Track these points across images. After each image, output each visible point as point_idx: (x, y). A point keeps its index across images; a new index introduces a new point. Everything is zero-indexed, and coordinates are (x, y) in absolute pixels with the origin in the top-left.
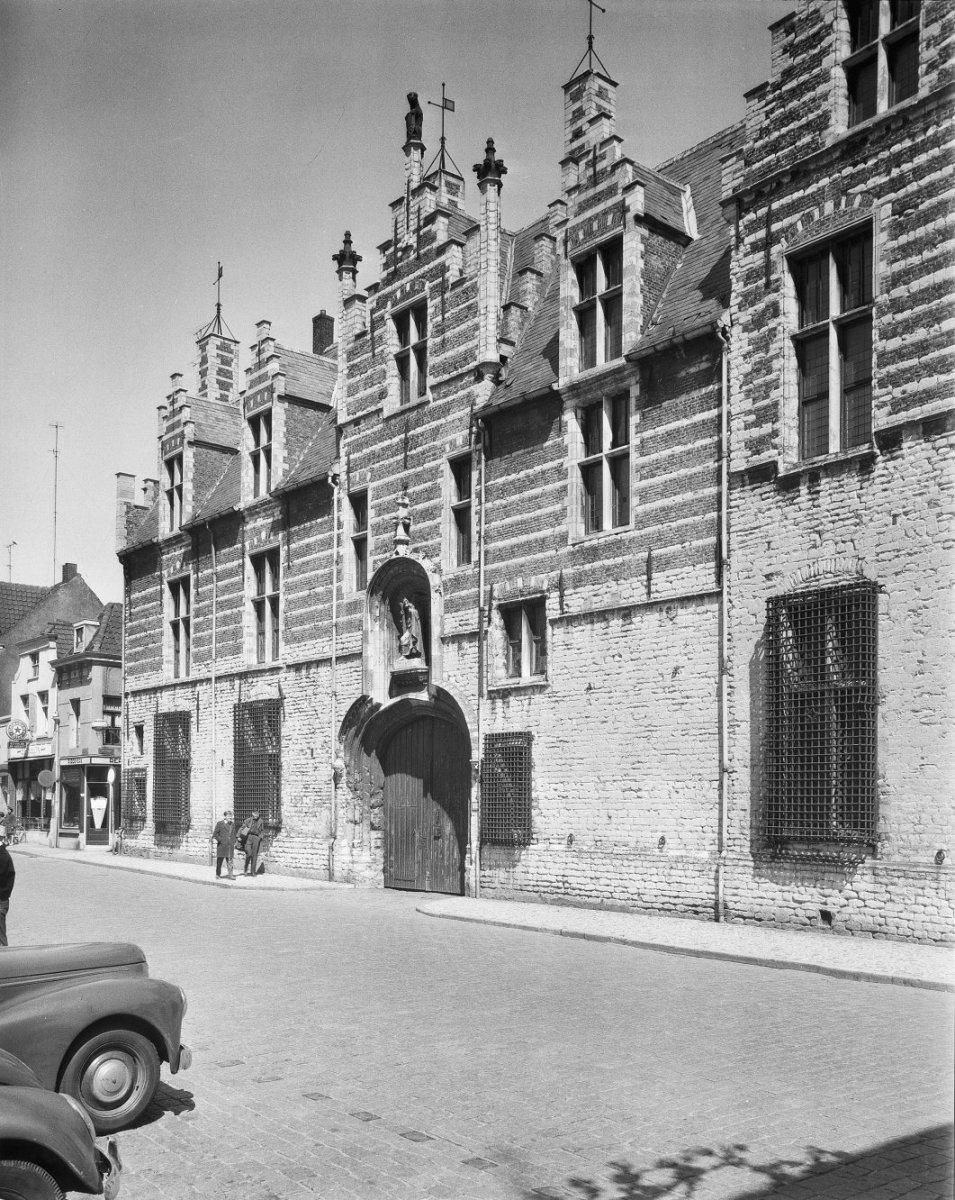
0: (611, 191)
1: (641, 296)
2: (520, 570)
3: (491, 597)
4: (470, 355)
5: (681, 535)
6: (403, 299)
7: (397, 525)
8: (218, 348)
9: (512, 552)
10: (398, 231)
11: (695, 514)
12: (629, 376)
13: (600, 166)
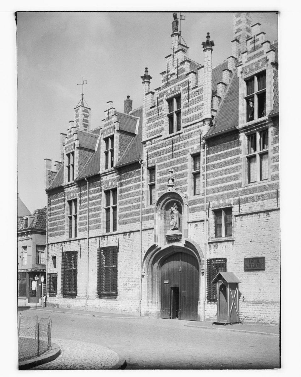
0: (261, 53)
1: (273, 93)
2: (221, 197)
3: (209, 207)
4: (200, 115)
6: (170, 94)
7: (169, 179)
8: (83, 111)
10: (169, 68)
13: (256, 44)
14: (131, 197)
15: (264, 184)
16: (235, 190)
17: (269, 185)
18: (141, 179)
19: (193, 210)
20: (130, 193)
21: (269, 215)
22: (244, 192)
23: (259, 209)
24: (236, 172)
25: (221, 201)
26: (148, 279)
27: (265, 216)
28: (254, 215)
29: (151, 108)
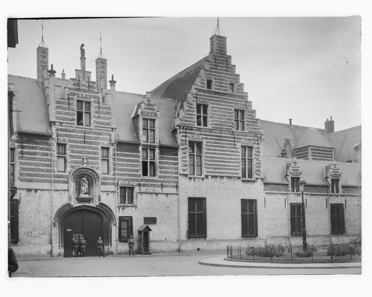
2: (127, 180)
5: (169, 182)
12: (157, 148)
15: (154, 179)
16: (136, 178)
17: (157, 180)
19: (103, 184)
20: (36, 158)
22: (142, 180)
23: (152, 191)
24: (137, 167)
26: (59, 228)
27: (155, 196)
28: (149, 194)
29: (62, 99)
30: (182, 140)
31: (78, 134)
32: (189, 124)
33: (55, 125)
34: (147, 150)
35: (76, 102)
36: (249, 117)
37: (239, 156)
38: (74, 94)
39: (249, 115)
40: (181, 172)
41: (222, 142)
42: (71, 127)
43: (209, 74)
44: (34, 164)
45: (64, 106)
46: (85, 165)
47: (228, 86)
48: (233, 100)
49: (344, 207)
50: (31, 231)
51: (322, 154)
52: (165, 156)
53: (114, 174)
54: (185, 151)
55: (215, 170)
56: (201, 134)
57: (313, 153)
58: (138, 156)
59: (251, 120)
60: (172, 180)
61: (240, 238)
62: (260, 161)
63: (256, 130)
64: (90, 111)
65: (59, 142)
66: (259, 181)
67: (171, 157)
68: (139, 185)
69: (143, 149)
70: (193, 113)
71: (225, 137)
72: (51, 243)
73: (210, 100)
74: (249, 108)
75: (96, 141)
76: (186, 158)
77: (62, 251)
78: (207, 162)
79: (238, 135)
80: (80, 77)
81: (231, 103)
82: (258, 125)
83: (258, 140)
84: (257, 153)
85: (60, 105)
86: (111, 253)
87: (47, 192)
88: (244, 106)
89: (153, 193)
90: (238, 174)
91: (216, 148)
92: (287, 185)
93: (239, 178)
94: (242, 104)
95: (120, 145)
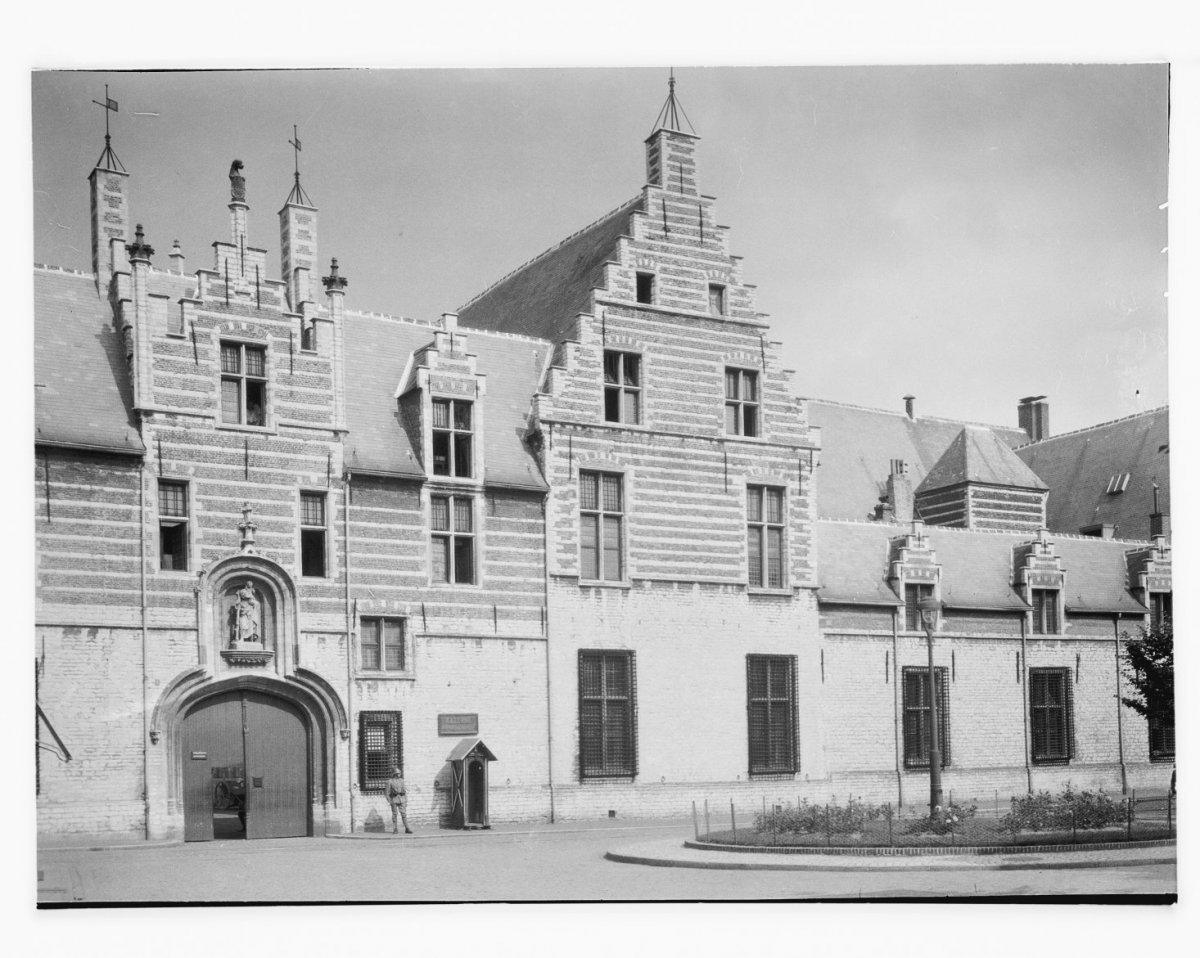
2: (382, 595)
3: (355, 609)
5: (516, 601)
9: (376, 579)
11: (525, 591)
14: (94, 535)
16: (413, 588)
17: (481, 596)
18: (136, 498)
19: (311, 608)
20: (94, 527)
21: (480, 643)
22: (432, 596)
23: (462, 631)
25: (383, 603)
26: (169, 748)
27: (474, 645)
28: (452, 640)
30: (558, 469)
31: (227, 450)
32: (579, 415)
33: (154, 422)
34: (446, 499)
35: (217, 346)
36: (772, 392)
37: (741, 518)
38: (212, 322)
39: (772, 386)
40: (555, 568)
41: (685, 472)
42: (202, 426)
43: (645, 256)
44: (86, 547)
45: (181, 359)
46: (248, 547)
47: (706, 293)
48: (719, 338)
49: (1074, 678)
50: (81, 758)
51: (1009, 507)
52: (503, 519)
53: (344, 578)
54: (567, 503)
55: (663, 564)
56: (618, 449)
57: (980, 505)
58: (417, 520)
59: (778, 403)
60: (526, 594)
61: (744, 776)
62: (809, 532)
63: (795, 435)
64: (263, 375)
65: (165, 475)
66: (804, 595)
67: (524, 521)
68: (423, 612)
69: (434, 497)
70: (593, 381)
71: (696, 457)
72: (144, 796)
73: (647, 338)
74: (772, 363)
75: (284, 471)
76: (571, 526)
77: (179, 820)
78: (637, 539)
79: (736, 451)
80: (229, 266)
81: (714, 348)
82: (800, 417)
83: (800, 467)
84: (797, 509)
85: (166, 357)
86: (328, 829)
87: (127, 635)
88: (756, 359)
89: (465, 637)
90: (736, 574)
91: (666, 494)
92: (893, 610)
93: (741, 586)
94: (750, 351)
95: (361, 480)
